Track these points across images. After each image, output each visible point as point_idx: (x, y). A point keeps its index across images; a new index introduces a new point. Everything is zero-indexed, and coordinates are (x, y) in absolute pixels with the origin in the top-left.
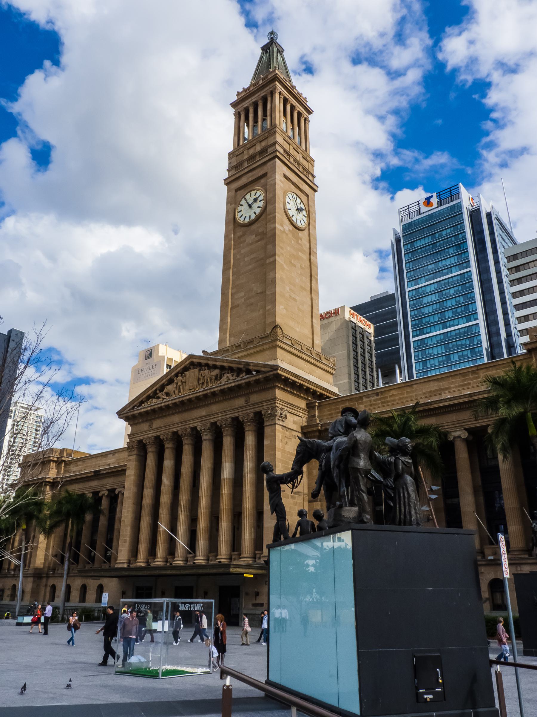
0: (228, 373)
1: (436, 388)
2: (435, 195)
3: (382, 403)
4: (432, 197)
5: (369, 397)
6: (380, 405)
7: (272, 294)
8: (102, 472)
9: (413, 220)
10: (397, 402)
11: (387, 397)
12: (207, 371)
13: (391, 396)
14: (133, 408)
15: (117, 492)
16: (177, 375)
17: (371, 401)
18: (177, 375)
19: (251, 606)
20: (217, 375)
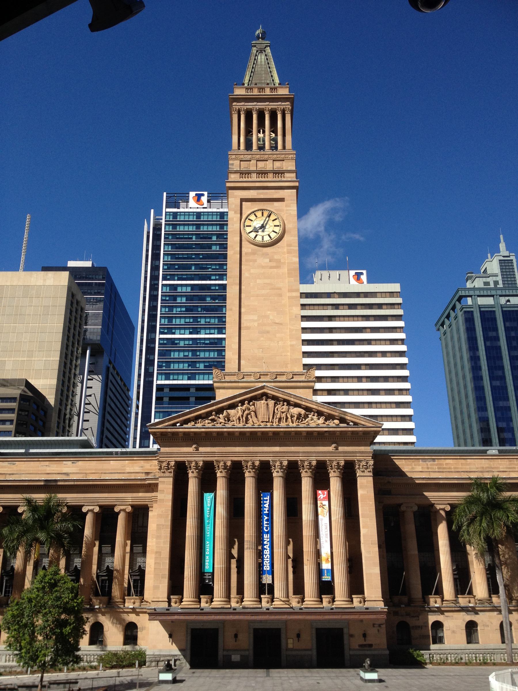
0: (314, 415)
1: (487, 466)
2: (206, 193)
3: (438, 468)
4: (203, 195)
5: (425, 462)
6: (437, 470)
7: (296, 330)
8: (59, 483)
9: (178, 210)
10: (453, 470)
11: (443, 464)
12: (285, 407)
13: (447, 464)
14: (174, 425)
15: (84, 510)
16: (242, 402)
17: (427, 465)
18: (242, 402)
19: (357, 647)
20: (300, 415)
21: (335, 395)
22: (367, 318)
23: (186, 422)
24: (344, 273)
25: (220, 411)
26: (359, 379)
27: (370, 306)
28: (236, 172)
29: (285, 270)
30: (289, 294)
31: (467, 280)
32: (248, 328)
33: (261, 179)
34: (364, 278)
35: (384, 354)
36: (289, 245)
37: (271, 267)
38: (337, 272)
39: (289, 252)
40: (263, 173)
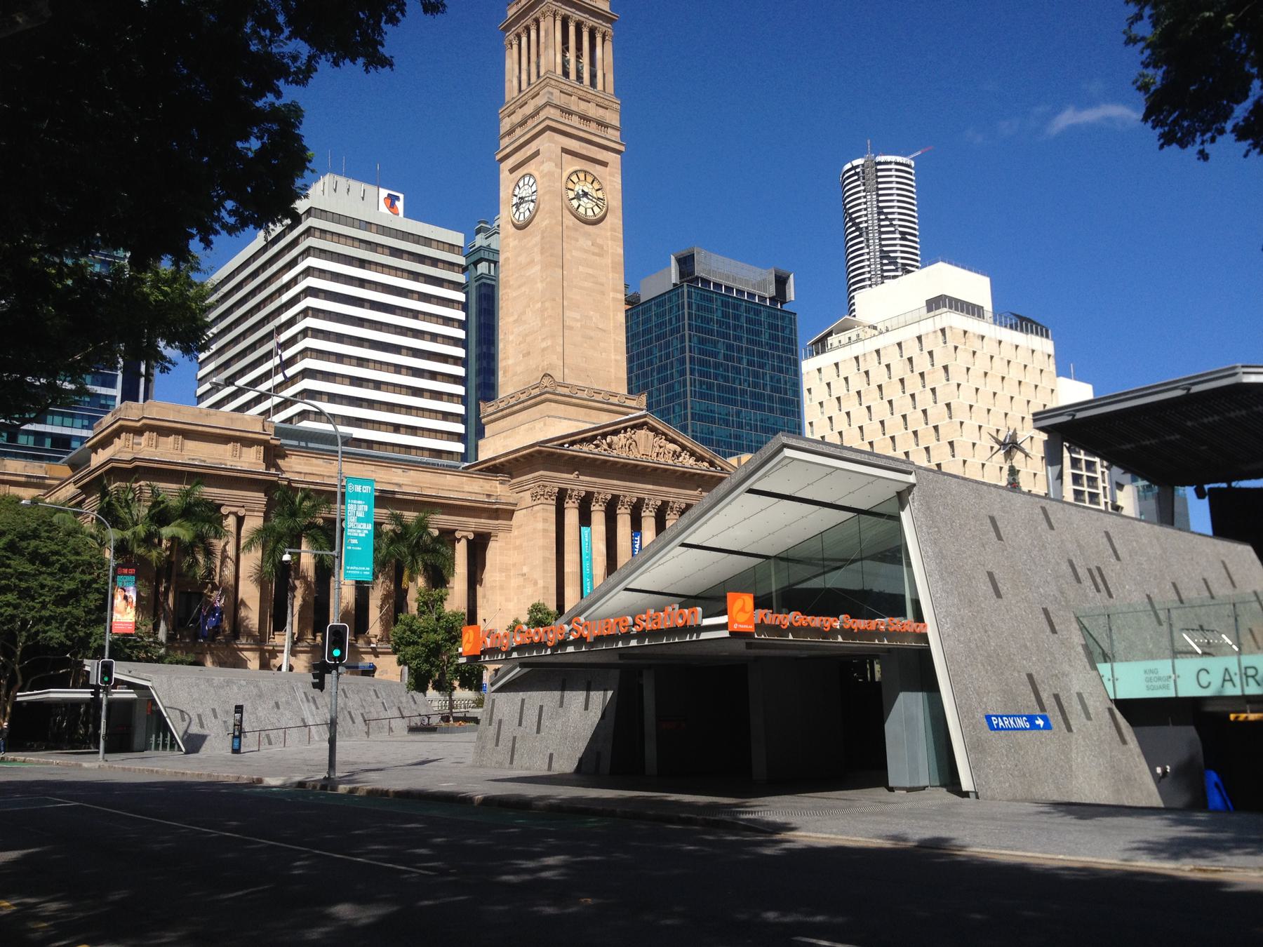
12: (663, 442)
14: (562, 445)
16: (625, 429)
20: (675, 452)
21: (361, 386)
22: (415, 276)
23: (572, 443)
24: (371, 189)
25: (604, 436)
26: (398, 369)
27: (421, 259)
28: (556, 107)
29: (608, 261)
30: (612, 295)
31: (478, 232)
32: (571, 328)
33: (581, 126)
34: (400, 205)
35: (434, 337)
36: (613, 230)
37: (594, 254)
38: (363, 185)
39: (614, 239)
40: (585, 118)
